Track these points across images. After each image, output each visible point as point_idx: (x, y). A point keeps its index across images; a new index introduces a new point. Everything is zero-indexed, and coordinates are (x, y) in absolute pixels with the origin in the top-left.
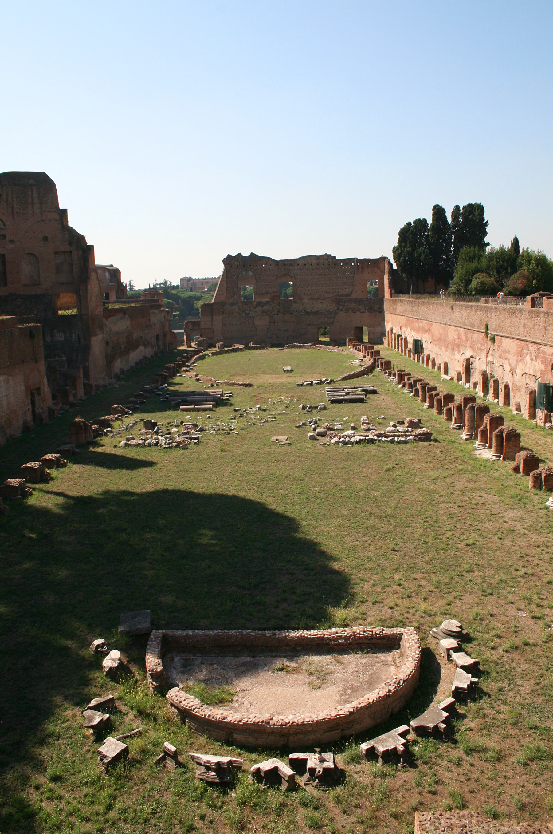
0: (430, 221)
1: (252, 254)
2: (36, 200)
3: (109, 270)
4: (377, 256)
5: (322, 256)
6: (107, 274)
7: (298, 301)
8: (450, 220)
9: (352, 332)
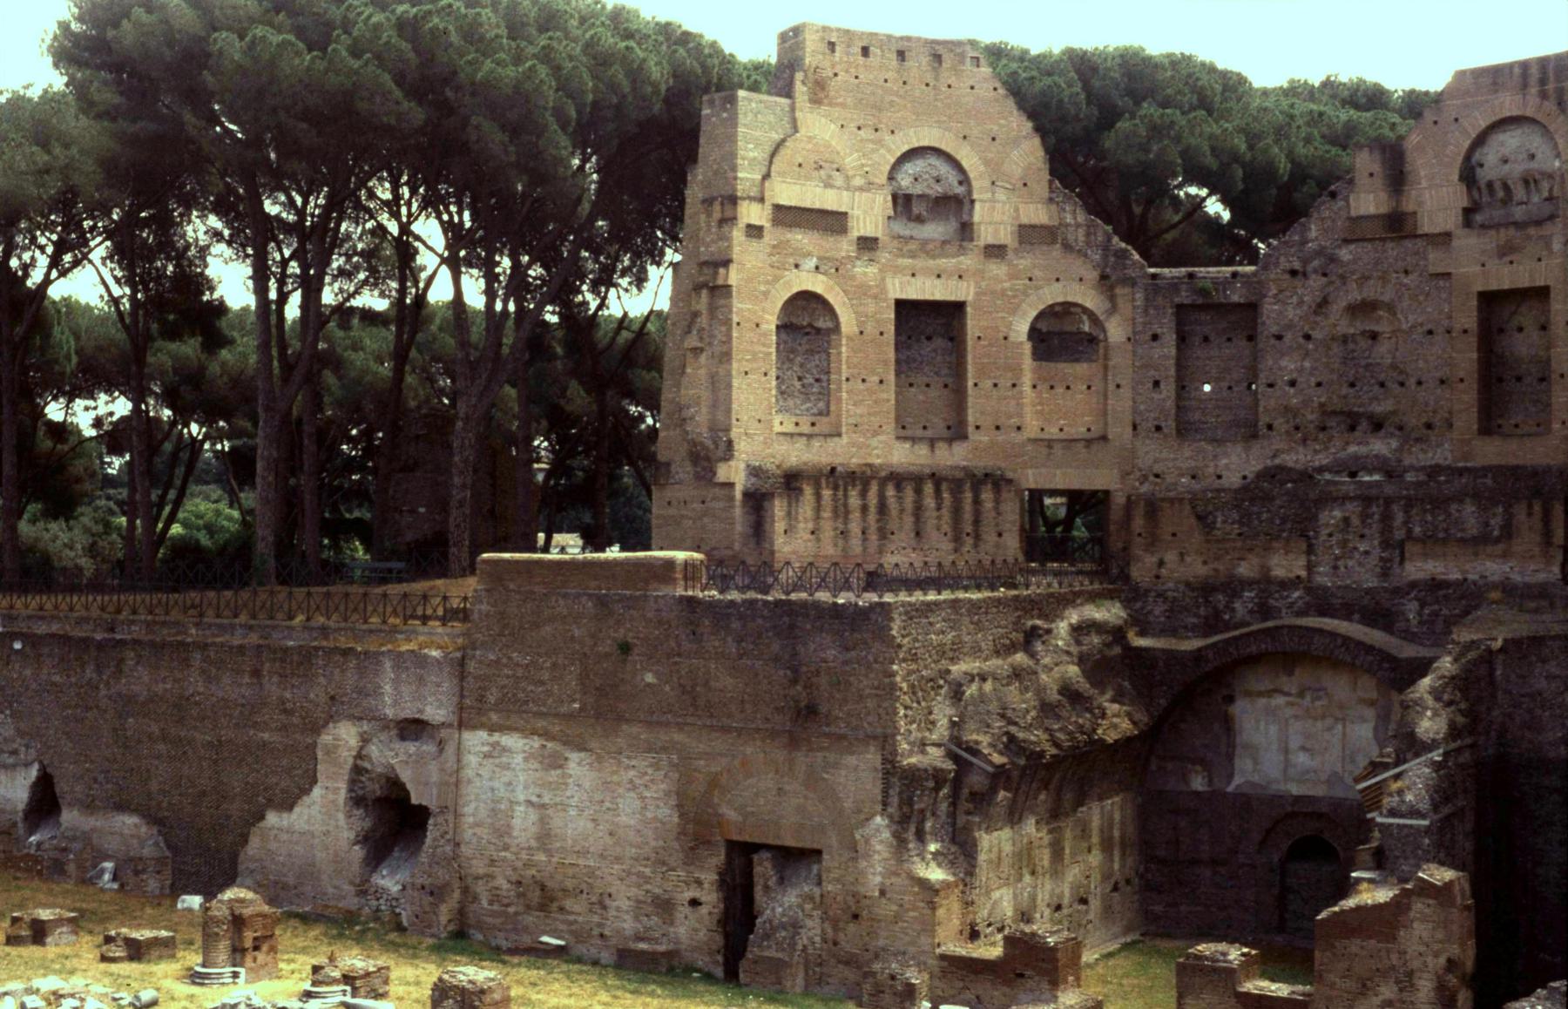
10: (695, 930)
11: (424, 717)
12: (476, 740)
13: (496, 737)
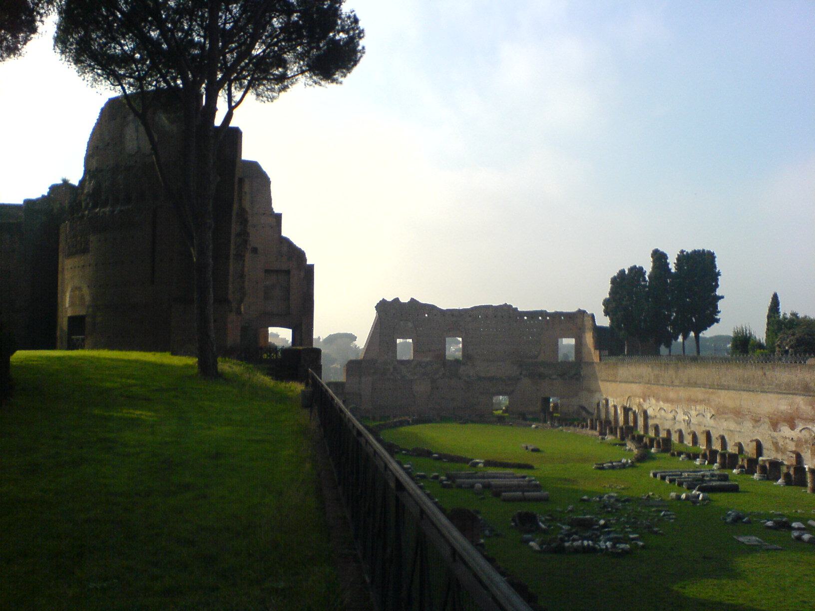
1: (412, 299)
4: (573, 309)
8: (673, 268)
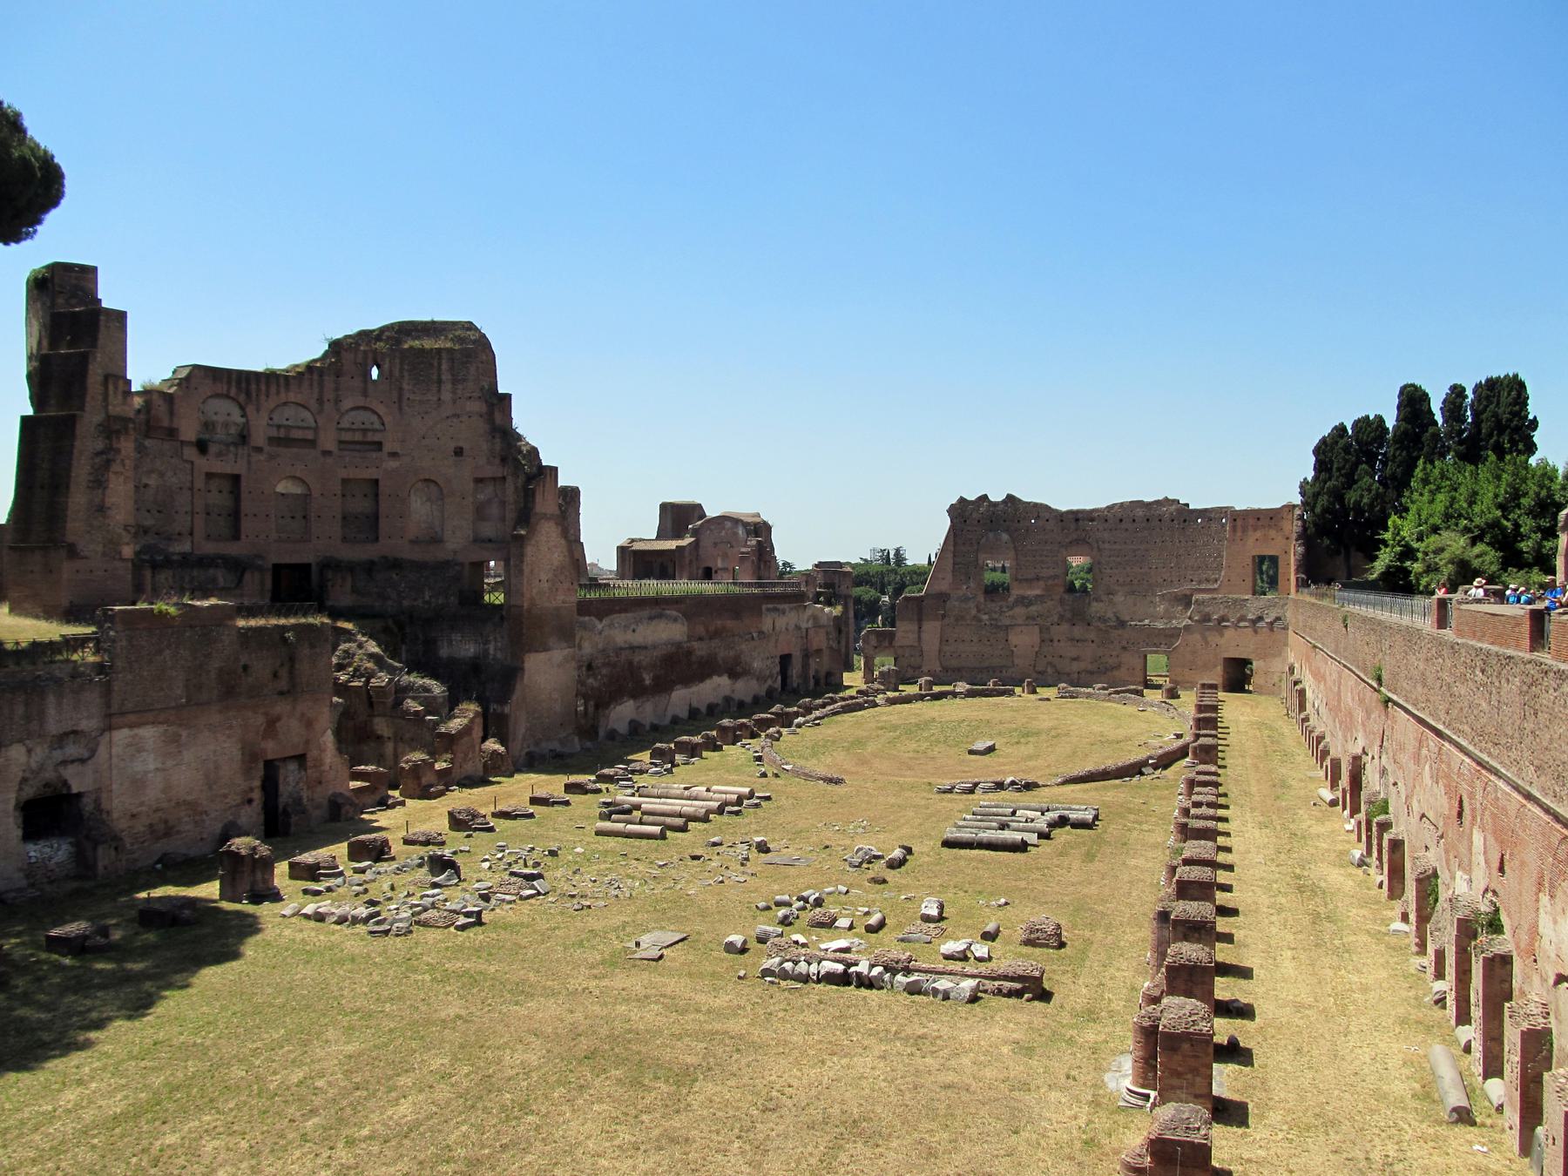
0: (1390, 423)
1: (1010, 498)
2: (446, 377)
3: (745, 525)
5: (1157, 502)
6: (741, 531)
7: (1104, 598)
9: (1220, 669)
10: (251, 817)
11: (79, 729)
12: (121, 736)
13: (136, 731)
